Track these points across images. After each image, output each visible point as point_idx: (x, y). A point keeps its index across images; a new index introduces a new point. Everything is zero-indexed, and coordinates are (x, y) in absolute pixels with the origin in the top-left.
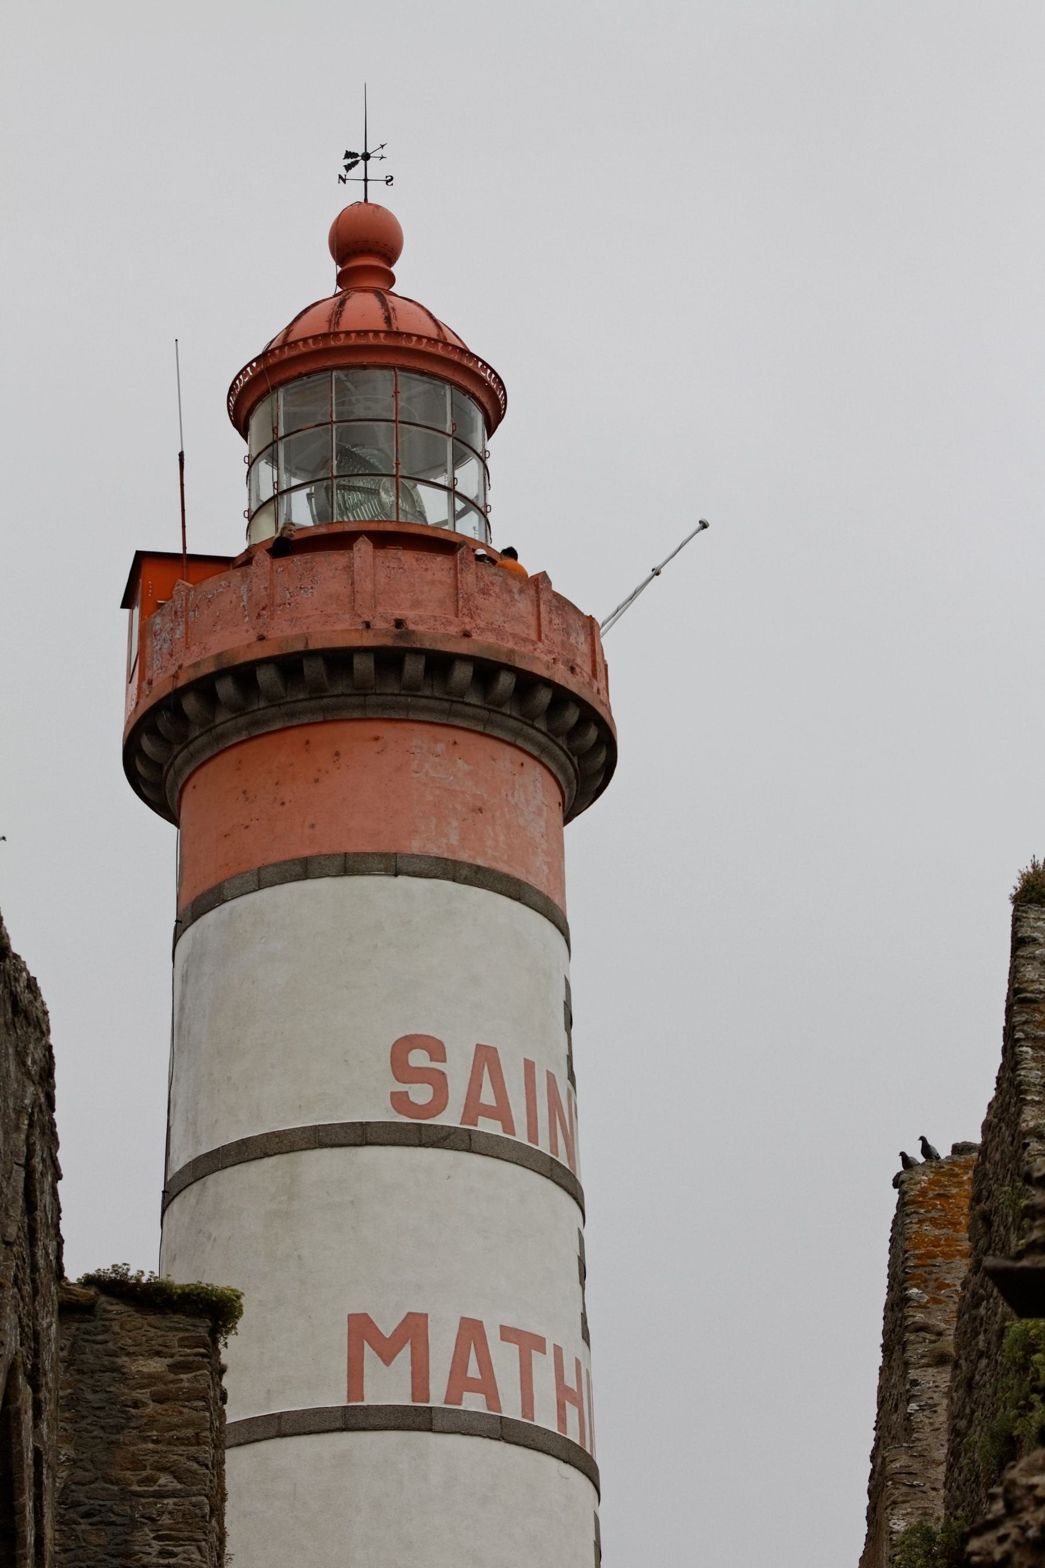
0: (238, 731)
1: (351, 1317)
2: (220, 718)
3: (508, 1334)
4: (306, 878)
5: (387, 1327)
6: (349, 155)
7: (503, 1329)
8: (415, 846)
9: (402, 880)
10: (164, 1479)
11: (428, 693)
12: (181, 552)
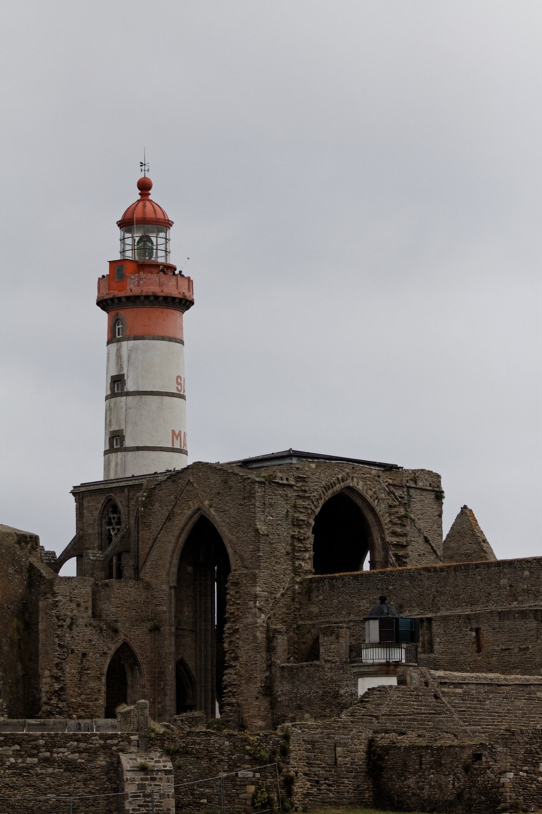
6: (141, 163)
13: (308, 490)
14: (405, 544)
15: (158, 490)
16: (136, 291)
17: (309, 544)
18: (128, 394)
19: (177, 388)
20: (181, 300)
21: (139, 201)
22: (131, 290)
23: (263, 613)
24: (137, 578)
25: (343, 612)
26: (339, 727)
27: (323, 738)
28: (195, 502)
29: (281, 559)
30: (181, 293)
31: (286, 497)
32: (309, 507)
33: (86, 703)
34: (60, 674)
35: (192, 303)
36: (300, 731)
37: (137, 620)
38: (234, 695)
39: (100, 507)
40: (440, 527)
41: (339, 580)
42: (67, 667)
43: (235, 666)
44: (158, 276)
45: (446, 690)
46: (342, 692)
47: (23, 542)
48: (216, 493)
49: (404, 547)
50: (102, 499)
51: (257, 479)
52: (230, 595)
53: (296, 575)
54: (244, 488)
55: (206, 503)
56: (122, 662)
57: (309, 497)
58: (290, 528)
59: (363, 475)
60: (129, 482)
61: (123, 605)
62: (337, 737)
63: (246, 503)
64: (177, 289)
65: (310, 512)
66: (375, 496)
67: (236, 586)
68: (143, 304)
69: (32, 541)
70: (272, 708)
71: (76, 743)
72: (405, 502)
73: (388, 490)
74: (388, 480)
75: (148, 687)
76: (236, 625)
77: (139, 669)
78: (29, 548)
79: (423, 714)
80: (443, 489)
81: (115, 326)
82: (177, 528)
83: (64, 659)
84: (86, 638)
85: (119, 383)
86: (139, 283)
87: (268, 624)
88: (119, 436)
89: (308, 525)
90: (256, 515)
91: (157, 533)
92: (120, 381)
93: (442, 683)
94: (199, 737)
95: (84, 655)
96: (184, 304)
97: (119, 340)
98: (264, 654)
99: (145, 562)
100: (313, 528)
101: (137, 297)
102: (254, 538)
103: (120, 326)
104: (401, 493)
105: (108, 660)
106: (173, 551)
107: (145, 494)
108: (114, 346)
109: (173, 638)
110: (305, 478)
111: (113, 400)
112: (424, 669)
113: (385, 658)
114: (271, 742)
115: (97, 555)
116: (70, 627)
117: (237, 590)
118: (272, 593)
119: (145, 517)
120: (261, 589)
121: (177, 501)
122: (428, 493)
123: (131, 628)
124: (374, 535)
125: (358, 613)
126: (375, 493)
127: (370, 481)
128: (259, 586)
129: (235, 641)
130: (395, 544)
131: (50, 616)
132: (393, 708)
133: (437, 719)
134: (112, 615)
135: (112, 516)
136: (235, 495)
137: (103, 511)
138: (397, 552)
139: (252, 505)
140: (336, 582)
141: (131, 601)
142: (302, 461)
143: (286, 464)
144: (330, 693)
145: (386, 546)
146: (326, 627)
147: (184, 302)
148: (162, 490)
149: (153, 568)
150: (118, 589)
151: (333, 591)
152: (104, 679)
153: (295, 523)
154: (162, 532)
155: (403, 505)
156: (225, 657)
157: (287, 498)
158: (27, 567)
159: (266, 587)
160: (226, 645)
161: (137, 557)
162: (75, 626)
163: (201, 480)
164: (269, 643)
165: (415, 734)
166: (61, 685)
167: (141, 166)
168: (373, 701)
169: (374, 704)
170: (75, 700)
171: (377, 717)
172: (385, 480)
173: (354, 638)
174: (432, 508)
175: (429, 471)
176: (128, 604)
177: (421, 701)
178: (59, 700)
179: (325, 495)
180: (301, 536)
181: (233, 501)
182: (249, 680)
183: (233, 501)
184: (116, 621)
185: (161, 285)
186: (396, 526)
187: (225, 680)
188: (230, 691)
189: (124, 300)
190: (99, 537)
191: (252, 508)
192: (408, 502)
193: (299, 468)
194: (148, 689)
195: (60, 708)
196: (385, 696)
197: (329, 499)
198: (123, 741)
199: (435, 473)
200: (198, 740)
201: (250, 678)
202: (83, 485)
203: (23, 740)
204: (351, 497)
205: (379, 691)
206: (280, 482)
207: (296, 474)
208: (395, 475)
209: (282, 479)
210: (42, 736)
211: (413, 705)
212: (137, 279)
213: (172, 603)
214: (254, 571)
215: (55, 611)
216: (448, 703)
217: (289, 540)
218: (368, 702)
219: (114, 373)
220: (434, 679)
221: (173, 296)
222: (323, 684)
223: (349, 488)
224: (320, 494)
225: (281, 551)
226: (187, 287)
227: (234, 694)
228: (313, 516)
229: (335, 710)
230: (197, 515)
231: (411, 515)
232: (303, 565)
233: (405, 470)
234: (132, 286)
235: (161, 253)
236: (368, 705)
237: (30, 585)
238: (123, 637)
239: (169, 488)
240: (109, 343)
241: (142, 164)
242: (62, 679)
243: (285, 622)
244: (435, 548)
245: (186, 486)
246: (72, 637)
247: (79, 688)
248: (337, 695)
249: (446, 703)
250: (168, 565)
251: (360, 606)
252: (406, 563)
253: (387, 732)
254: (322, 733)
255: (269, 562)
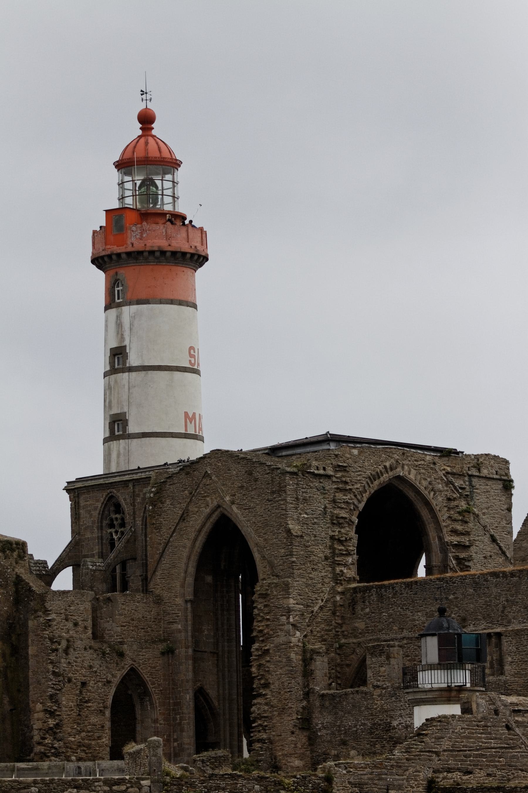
0: (154, 262)
5: (191, 415)
6: (142, 91)
13: (349, 481)
14: (467, 544)
15: (169, 484)
16: (139, 246)
17: (353, 546)
18: (131, 369)
19: (190, 361)
20: (193, 255)
21: (140, 137)
22: (133, 244)
23: (298, 630)
24: (146, 590)
25: (395, 628)
26: (392, 766)
27: (372, 779)
28: (213, 498)
29: (319, 565)
30: (193, 247)
31: (323, 491)
32: (351, 501)
33: (86, 741)
34: (55, 708)
35: (206, 259)
36: (345, 772)
37: (146, 642)
38: (265, 730)
39: (100, 506)
40: (510, 523)
41: (389, 589)
42: (64, 699)
43: (265, 695)
44: (164, 227)
45: (520, 719)
46: (395, 723)
47: (8, 550)
48: (239, 487)
49: (466, 547)
50: (102, 496)
51: (288, 469)
52: (259, 610)
53: (337, 583)
54: (272, 481)
55: (228, 498)
56: (130, 692)
57: (351, 489)
58: (328, 527)
59: (415, 462)
60: (134, 475)
61: (129, 623)
62: (389, 779)
63: (275, 498)
64: (188, 242)
65: (352, 508)
66: (431, 487)
67: (265, 598)
68: (147, 261)
69: (18, 548)
70: (310, 745)
71: (75, 790)
72: (467, 493)
73: (445, 479)
74: (446, 467)
75: (162, 722)
76: (266, 646)
77: (150, 700)
78: (15, 557)
79: (493, 748)
80: (513, 477)
81: (113, 288)
82: (193, 530)
83: (59, 690)
84: (86, 664)
85: (120, 356)
86: (141, 236)
87: (304, 643)
88: (121, 420)
89: (350, 523)
90: (287, 513)
91: (169, 536)
92: (121, 354)
93: (514, 711)
94: (224, 780)
95: (84, 684)
96: (197, 261)
97: (119, 305)
98: (300, 679)
99: (154, 572)
100: (357, 527)
101: (140, 253)
102: (285, 540)
103: (120, 288)
104: (462, 482)
105: (113, 690)
106: (189, 558)
107: (153, 490)
108: (113, 312)
109: (190, 662)
110: (346, 467)
111: (113, 377)
112: (493, 694)
113: (446, 682)
114: (310, 785)
115: (97, 564)
116: (66, 651)
117: (266, 603)
118: (308, 606)
119: (155, 517)
120: (295, 602)
121: (192, 497)
122: (494, 482)
123: (140, 652)
124: (430, 534)
125: (412, 628)
126: (430, 483)
127: (424, 468)
128: (293, 598)
129: (265, 665)
130: (456, 544)
131: (42, 637)
132: (457, 742)
133: (509, 755)
134: (117, 636)
135: (114, 516)
136: (262, 488)
137: (103, 511)
138: (458, 554)
139: (282, 500)
140: (386, 591)
141: (139, 618)
142: (341, 447)
143: (322, 450)
144: (380, 725)
145: (444, 547)
146: (373, 646)
147: (196, 257)
148: (174, 484)
149: (164, 578)
150: (123, 604)
151: (381, 603)
152: (108, 713)
153: (335, 522)
154: (174, 535)
155: (464, 498)
156: (253, 683)
157: (325, 492)
158: (13, 579)
159: (301, 599)
160: (254, 669)
161: (145, 565)
162: (72, 650)
163: (220, 472)
164: (305, 666)
165: (483, 773)
166: (57, 721)
167: (142, 95)
168: (433, 734)
169: (433, 737)
170: (73, 739)
171: (437, 754)
172: (442, 468)
173: (408, 658)
174: (500, 501)
175: (495, 456)
176: (135, 622)
177: (490, 733)
178: (55, 738)
179: (370, 486)
180: (342, 537)
181: (259, 496)
182: (283, 711)
183: (259, 496)
184: (122, 643)
185: (168, 237)
186: (456, 523)
187: (254, 711)
188: (260, 725)
189: (124, 256)
190: (98, 542)
191: (282, 505)
192: (471, 494)
193: (338, 454)
194: (161, 724)
195: (55, 748)
196: (447, 727)
197: (376, 492)
198: (132, 787)
199: (502, 458)
200: (222, 784)
201: (284, 709)
202: (79, 480)
203: (12, 788)
204: (402, 489)
205: (440, 721)
206: (316, 472)
207: (334, 463)
208: (454, 462)
209: (318, 469)
210: (35, 782)
211: (481, 738)
212: (139, 231)
213: (188, 620)
214: (286, 579)
215: (47, 632)
216: (523, 734)
217: (328, 542)
218: (426, 735)
219: (114, 344)
220: (505, 706)
221: (183, 250)
222: (372, 715)
223: (399, 478)
224: (365, 485)
225: (318, 555)
226: (199, 239)
227: (265, 729)
228: (356, 513)
229: (386, 745)
230: (217, 513)
231: (474, 509)
232: (345, 571)
233: (466, 455)
234: (133, 240)
235: (168, 200)
236: (426, 739)
237: (17, 602)
238: (131, 662)
239: (182, 482)
240: (107, 308)
241: (143, 93)
242: (58, 713)
243: (325, 640)
245: (202, 478)
246: (69, 663)
247: (78, 724)
248: (388, 728)
249: (521, 736)
250: (182, 574)
251: (414, 620)
252: (469, 567)
253: (449, 770)
254: (371, 773)
255: (304, 569)
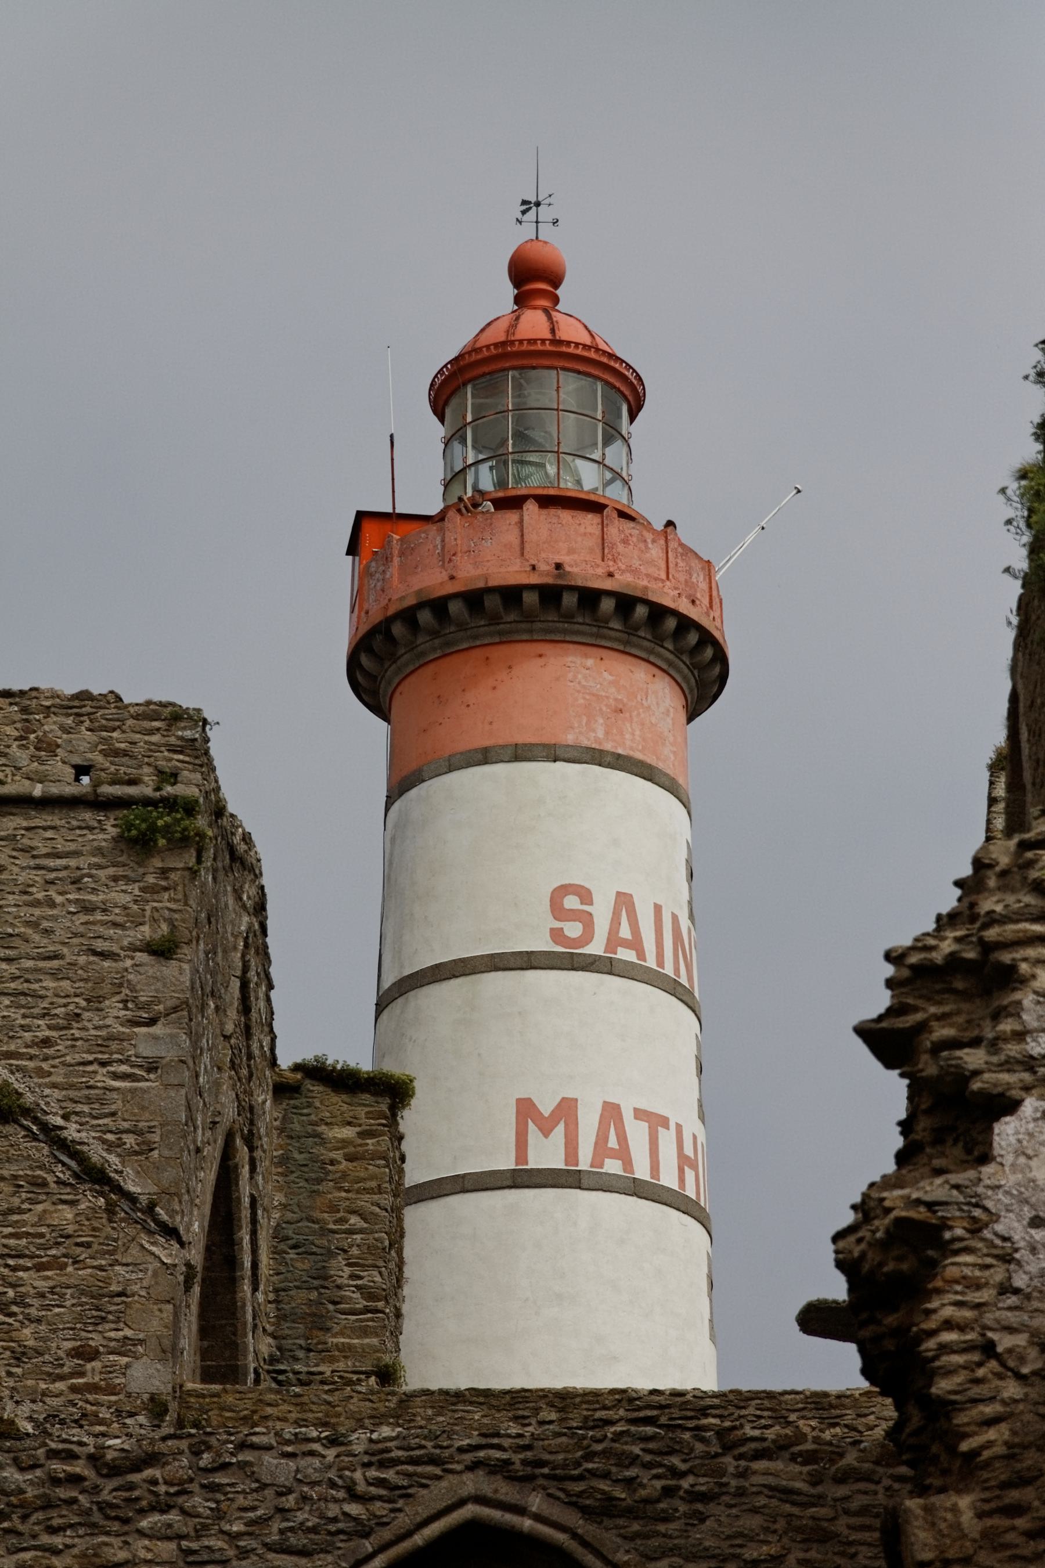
0: (434, 649)
1: (519, 1101)
2: (420, 640)
3: (640, 1114)
4: (486, 763)
5: (546, 1107)
7: (636, 1110)
8: (570, 739)
9: (559, 764)
10: (354, 1220)
11: (580, 620)
12: (390, 510)
64: (522, 554)
174: (87, 908)
185: (446, 557)
244: (96, 1153)
